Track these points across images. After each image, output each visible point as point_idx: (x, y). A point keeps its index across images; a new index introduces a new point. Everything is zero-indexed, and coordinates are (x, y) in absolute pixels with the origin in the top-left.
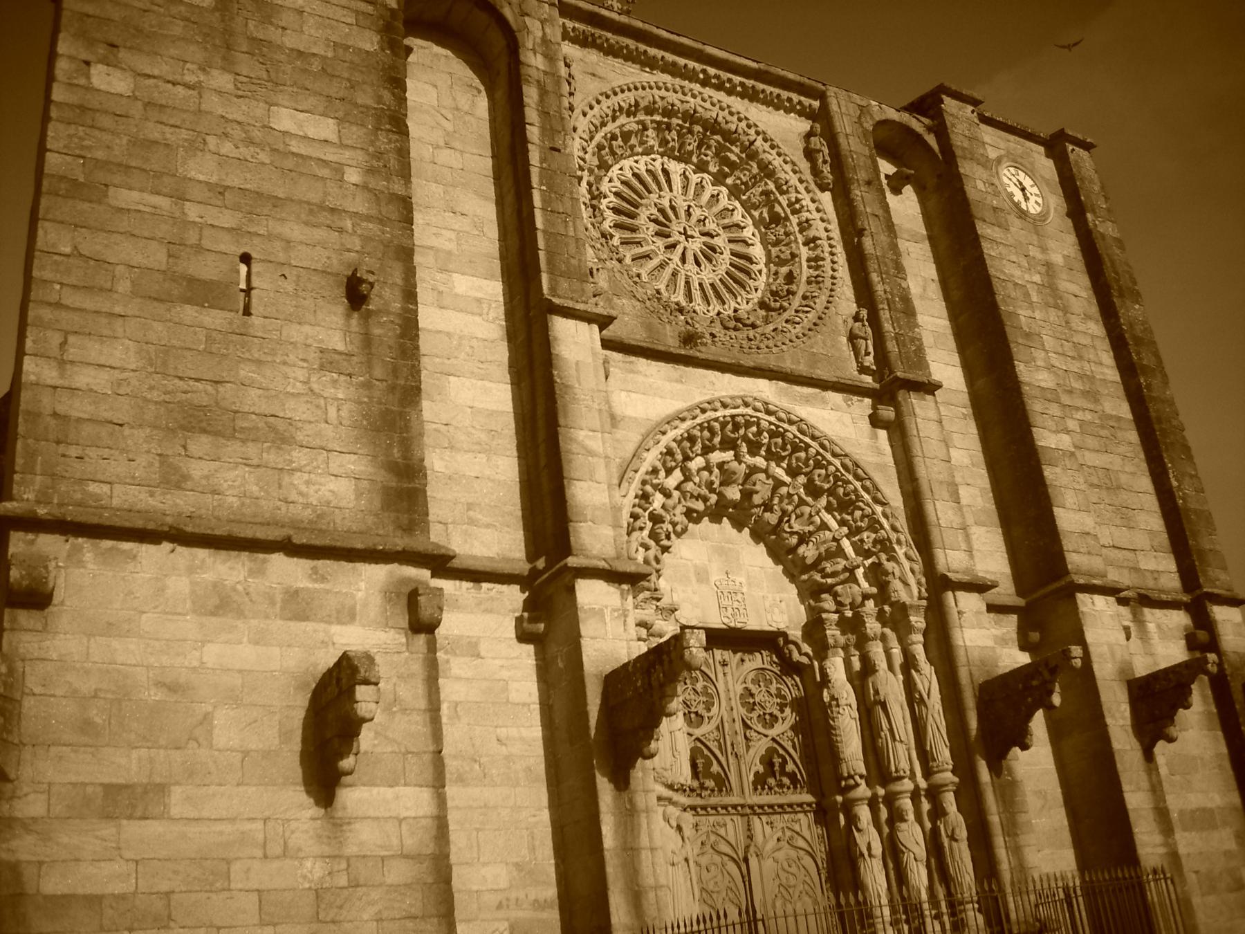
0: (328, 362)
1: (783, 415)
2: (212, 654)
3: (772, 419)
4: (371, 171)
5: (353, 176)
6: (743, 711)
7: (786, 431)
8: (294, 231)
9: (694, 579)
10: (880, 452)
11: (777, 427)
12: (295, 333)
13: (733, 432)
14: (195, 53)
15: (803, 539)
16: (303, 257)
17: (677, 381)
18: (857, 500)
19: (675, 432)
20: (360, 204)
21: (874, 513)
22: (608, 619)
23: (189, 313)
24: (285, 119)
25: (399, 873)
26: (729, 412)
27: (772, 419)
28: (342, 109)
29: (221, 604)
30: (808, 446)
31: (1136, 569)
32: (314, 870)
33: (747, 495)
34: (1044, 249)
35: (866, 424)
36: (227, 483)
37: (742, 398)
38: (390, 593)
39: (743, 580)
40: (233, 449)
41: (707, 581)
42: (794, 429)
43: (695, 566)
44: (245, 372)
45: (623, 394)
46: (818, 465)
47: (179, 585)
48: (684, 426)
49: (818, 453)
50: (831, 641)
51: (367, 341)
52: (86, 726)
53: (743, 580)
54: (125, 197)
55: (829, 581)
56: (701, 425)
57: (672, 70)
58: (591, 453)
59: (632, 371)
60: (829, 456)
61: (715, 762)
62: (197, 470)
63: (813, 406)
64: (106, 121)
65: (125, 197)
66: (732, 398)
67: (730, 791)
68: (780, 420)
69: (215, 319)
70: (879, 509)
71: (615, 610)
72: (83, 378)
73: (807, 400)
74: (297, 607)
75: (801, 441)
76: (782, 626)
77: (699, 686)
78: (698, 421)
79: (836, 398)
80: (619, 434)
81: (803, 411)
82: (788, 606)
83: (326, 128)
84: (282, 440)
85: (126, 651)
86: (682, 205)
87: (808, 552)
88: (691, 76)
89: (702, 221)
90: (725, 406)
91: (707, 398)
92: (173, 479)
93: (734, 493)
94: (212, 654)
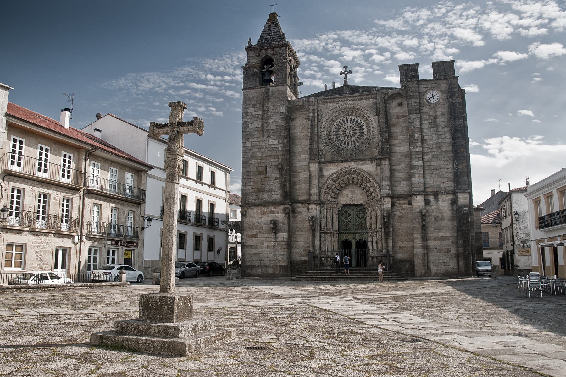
0: (277, 179)
2: (263, 219)
4: (283, 147)
5: (280, 149)
8: (272, 160)
12: (272, 176)
14: (259, 135)
16: (274, 164)
20: (281, 153)
23: (259, 176)
24: (271, 142)
25: (283, 243)
28: (278, 138)
29: (264, 213)
31: (440, 187)
32: (273, 243)
34: (435, 112)
35: (375, 167)
36: (265, 197)
38: (284, 210)
40: (265, 193)
44: (266, 182)
47: (259, 211)
51: (282, 174)
52: (250, 228)
54: (251, 161)
57: (342, 101)
62: (261, 197)
64: (248, 151)
65: (251, 161)
69: (263, 176)
72: (248, 188)
74: (272, 212)
79: (369, 162)
81: (361, 167)
83: (276, 142)
84: (271, 191)
85: (254, 219)
86: (349, 125)
87: (365, 190)
88: (347, 101)
89: (353, 128)
92: (258, 198)
94: (263, 219)
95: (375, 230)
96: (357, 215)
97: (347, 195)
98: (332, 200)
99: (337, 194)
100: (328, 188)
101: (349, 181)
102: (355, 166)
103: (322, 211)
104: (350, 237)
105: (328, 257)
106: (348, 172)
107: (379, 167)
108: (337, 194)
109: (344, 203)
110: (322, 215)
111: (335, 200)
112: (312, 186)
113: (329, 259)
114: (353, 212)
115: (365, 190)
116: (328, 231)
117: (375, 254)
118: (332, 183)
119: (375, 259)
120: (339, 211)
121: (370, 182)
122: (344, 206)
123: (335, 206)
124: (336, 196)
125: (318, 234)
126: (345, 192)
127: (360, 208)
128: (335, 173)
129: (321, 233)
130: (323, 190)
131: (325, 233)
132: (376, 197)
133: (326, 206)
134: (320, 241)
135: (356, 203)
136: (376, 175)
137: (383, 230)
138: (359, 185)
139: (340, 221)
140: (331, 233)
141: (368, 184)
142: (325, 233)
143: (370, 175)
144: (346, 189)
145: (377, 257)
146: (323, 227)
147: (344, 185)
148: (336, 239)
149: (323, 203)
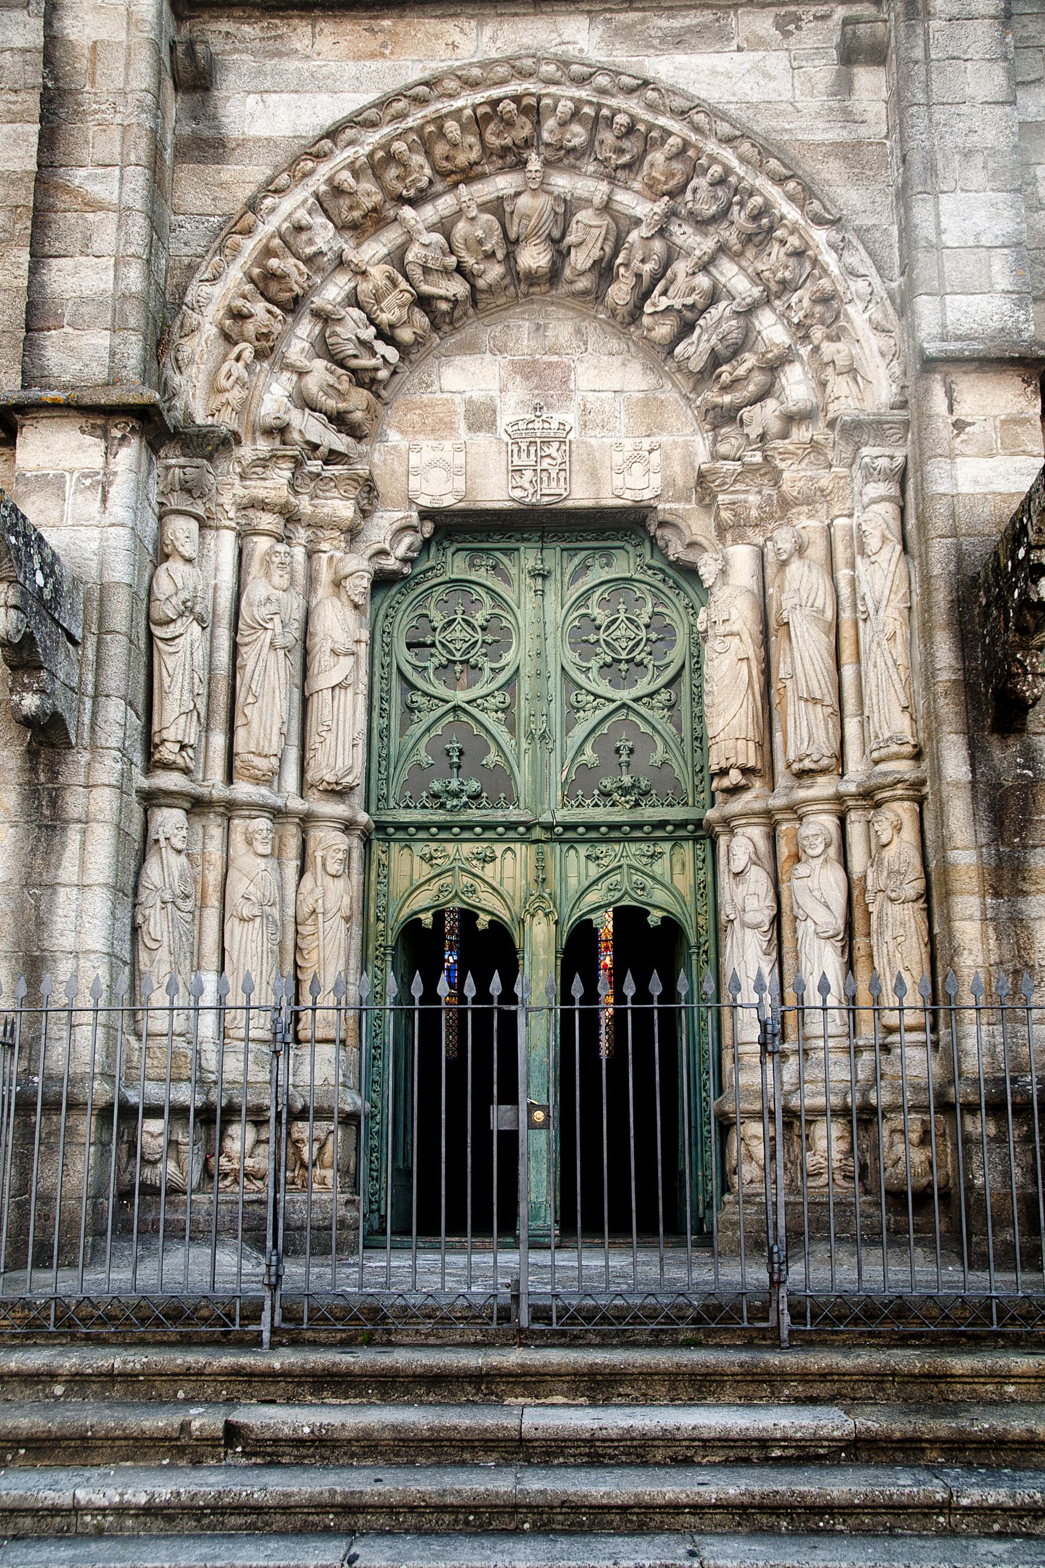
1: (602, 80)
3: (583, 94)
6: (570, 657)
7: (615, 112)
9: (462, 426)
10: (848, 117)
11: (599, 106)
13: (498, 135)
15: (686, 328)
17: (373, 56)
18: (771, 229)
19: (350, 152)
21: (808, 246)
22: (69, 488)
26: (479, 97)
27: (583, 94)
30: (667, 133)
33: (561, 253)
37: (507, 60)
39: (571, 418)
41: (490, 425)
42: (633, 105)
43: (470, 402)
45: (252, 99)
46: (695, 170)
48: (373, 138)
49: (686, 145)
50: (726, 515)
53: (571, 418)
55: (727, 399)
56: (419, 130)
58: (94, 206)
59: (279, 54)
60: (711, 146)
61: (493, 749)
63: (694, 48)
66: (484, 65)
67: (512, 800)
68: (602, 91)
70: (820, 236)
71: (86, 476)
73: (678, 41)
75: (651, 127)
76: (647, 495)
77: (479, 619)
78: (410, 122)
80: (228, 172)
81: (665, 67)
82: (666, 458)
87: (694, 350)
90: (473, 84)
91: (426, 75)
93: (534, 257)
95: (824, 787)
96: (583, 637)
97: (481, 418)
98: (312, 428)
99: (364, 379)
100: (265, 282)
101: (512, 244)
102: (597, 55)
103: (182, 531)
104: (501, 881)
105: (231, 1112)
106: (508, 132)
107: (870, 82)
108: (364, 379)
109: (440, 491)
110: (174, 581)
111: (340, 442)
112: (67, 221)
113: (240, 1138)
114: (538, 606)
115: (694, 350)
116: (243, 790)
117: (826, 1077)
118: (324, 236)
119: (828, 1142)
120: (382, 581)
121: (762, 231)
122: (458, 528)
123: (344, 509)
124: (358, 400)
125: (104, 802)
126: (466, 377)
127: (623, 565)
128: (360, 121)
129: (151, 799)
130: (214, 296)
131: (198, 806)
132: (839, 386)
133: (229, 486)
134: (130, 890)
135: (581, 496)
136: (850, 152)
137: (955, 765)
138: (620, 292)
139: (390, 695)
140: (277, 814)
141: (731, 275)
142: (198, 806)
143: (765, 150)
144: (471, 348)
145: (863, 1118)
146: (175, 723)
147: (457, 287)
148: (333, 893)
149: (211, 445)
